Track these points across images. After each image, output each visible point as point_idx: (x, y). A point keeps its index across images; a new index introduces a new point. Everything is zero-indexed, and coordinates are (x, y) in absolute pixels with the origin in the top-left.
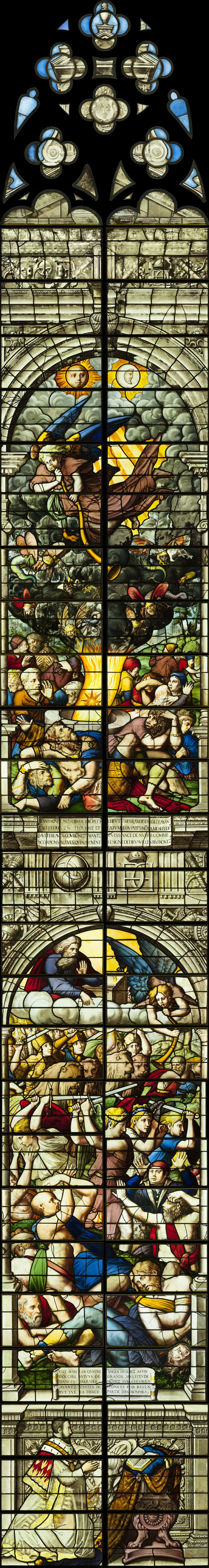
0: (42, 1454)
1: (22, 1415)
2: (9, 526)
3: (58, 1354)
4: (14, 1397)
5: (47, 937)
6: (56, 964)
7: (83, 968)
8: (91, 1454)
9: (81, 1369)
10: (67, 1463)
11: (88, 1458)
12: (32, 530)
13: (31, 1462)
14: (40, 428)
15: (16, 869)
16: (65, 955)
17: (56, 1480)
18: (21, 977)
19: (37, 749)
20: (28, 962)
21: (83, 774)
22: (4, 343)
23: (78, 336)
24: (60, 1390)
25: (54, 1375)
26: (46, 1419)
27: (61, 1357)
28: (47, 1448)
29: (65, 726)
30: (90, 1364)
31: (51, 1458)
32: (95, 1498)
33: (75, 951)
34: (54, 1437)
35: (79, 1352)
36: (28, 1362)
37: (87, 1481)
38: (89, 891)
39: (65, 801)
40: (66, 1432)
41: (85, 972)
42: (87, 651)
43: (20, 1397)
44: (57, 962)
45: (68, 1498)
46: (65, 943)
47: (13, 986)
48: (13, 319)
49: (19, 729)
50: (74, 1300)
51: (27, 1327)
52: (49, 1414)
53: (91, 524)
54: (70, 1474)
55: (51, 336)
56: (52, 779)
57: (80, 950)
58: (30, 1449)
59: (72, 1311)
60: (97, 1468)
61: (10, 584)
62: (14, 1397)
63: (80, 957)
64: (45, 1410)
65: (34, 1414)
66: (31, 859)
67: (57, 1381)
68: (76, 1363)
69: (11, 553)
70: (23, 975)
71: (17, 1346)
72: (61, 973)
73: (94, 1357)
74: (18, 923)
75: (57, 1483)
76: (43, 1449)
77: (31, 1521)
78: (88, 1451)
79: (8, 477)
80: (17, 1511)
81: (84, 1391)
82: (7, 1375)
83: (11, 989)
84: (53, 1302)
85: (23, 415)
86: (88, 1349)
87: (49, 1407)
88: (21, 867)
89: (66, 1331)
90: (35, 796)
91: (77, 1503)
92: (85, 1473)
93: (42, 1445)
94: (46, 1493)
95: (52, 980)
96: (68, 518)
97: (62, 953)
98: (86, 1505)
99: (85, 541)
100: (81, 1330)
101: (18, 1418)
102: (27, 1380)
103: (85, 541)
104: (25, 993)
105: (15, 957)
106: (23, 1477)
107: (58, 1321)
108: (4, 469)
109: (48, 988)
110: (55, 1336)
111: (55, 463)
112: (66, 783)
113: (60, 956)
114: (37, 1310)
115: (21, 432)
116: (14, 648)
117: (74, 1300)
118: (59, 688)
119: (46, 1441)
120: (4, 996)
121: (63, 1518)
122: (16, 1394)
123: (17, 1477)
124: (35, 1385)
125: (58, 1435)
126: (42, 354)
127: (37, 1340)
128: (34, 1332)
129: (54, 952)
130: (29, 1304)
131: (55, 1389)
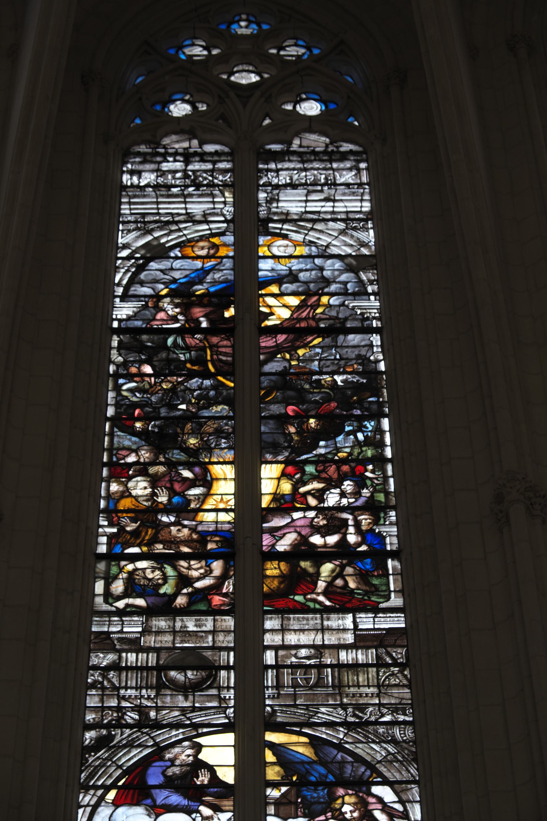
2: (120, 359)
5: (151, 743)
6: (163, 773)
7: (203, 778)
12: (148, 362)
14: (161, 286)
15: (108, 668)
16: (178, 762)
18: (107, 789)
19: (145, 549)
20: (119, 772)
21: (208, 573)
22: (121, 227)
23: (208, 222)
29: (185, 526)
33: (191, 758)
38: (214, 692)
39: (181, 601)
41: (206, 782)
42: (216, 460)
44: (165, 771)
46: (177, 750)
47: (95, 799)
48: (132, 212)
49: (122, 529)
53: (221, 357)
55: (177, 223)
56: (165, 578)
57: (200, 756)
61: (117, 405)
63: (198, 765)
66: (132, 657)
69: (121, 381)
70: (114, 786)
72: (170, 783)
74: (108, 726)
79: (120, 321)
83: (92, 803)
85: (142, 276)
88: (115, 666)
90: (139, 596)
95: (154, 792)
96: (193, 353)
97: (172, 761)
99: (212, 369)
103: (212, 369)
104: (113, 808)
105: (101, 766)
108: (116, 315)
109: (149, 801)
111: (177, 310)
112: (184, 581)
113: (169, 764)
115: (138, 289)
116: (119, 459)
118: (176, 494)
120: (81, 811)
126: (165, 235)
129: (162, 759)
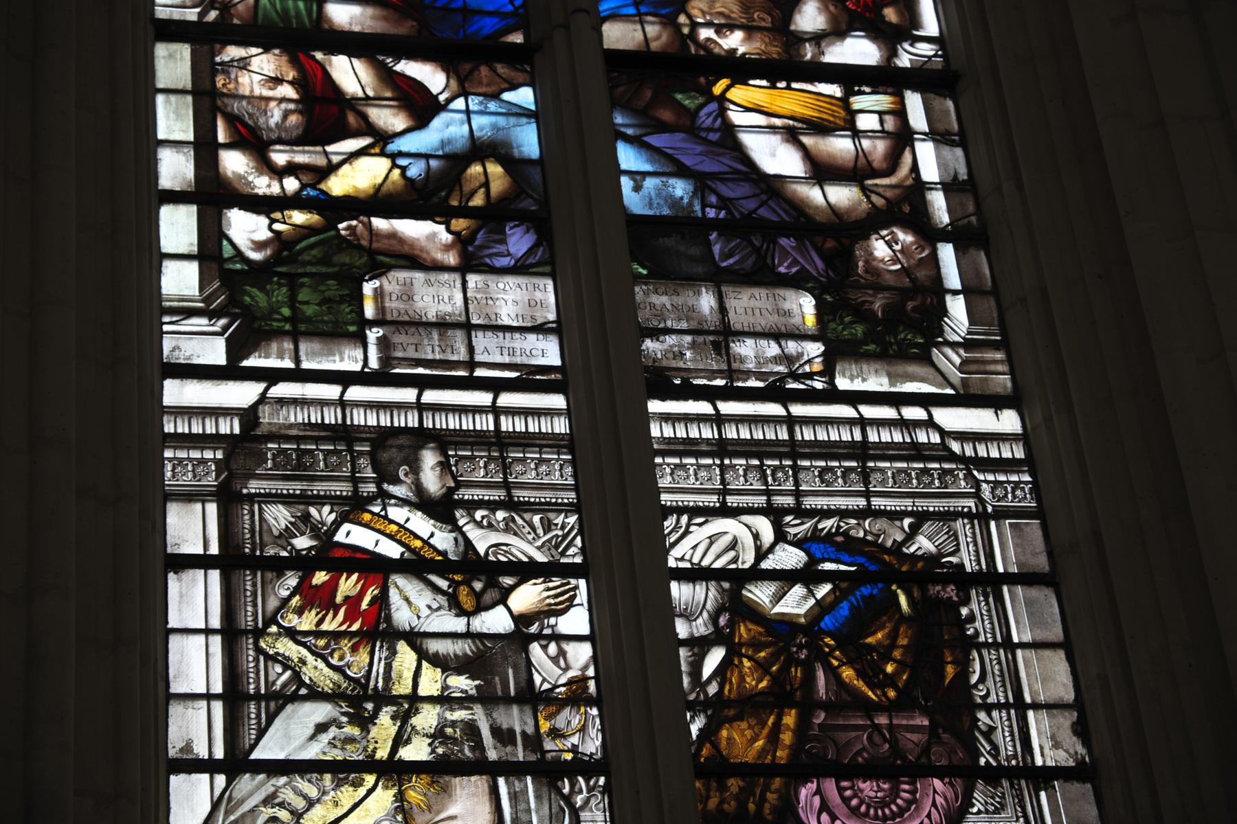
0: (338, 553)
1: (249, 416)
3: (379, 223)
4: (214, 352)
8: (541, 558)
9: (473, 280)
10: (443, 584)
11: (526, 571)
13: (292, 580)
17: (402, 646)
24: (397, 339)
25: (368, 288)
26: (344, 434)
27: (393, 235)
28: (355, 535)
30: (504, 262)
31: (374, 567)
32: (569, 718)
34: (384, 496)
35: (460, 224)
36: (259, 246)
37: (535, 648)
40: (432, 481)
43: (237, 349)
45: (459, 715)
50: (431, 77)
51: (254, 142)
52: (359, 418)
54: (458, 624)
58: (286, 535)
59: (422, 107)
60: (570, 603)
62: (214, 352)
64: (342, 403)
65: (297, 416)
67: (380, 309)
68: (452, 259)
71: (212, 195)
73: (519, 242)
75: (406, 657)
76: (340, 537)
77: (300, 804)
78: (525, 548)
80: (236, 763)
81: (488, 348)
82: (180, 280)
84: (350, 75)
86: (495, 216)
87: (356, 393)
89: (403, 162)
91: (496, 731)
92: (522, 620)
93: (337, 525)
94: (361, 701)
98: (534, 741)
100: (455, 161)
101: (227, 427)
102: (257, 297)
106: (259, 633)
107: (368, 128)
110: (360, 175)
114: (287, 91)
117: (431, 77)
119: (353, 508)
121: (446, 790)
122: (220, 344)
123: (231, 633)
124: (292, 320)
125: (399, 491)
127: (291, 184)
128: (280, 158)
130: (259, 73)
131: (373, 335)
